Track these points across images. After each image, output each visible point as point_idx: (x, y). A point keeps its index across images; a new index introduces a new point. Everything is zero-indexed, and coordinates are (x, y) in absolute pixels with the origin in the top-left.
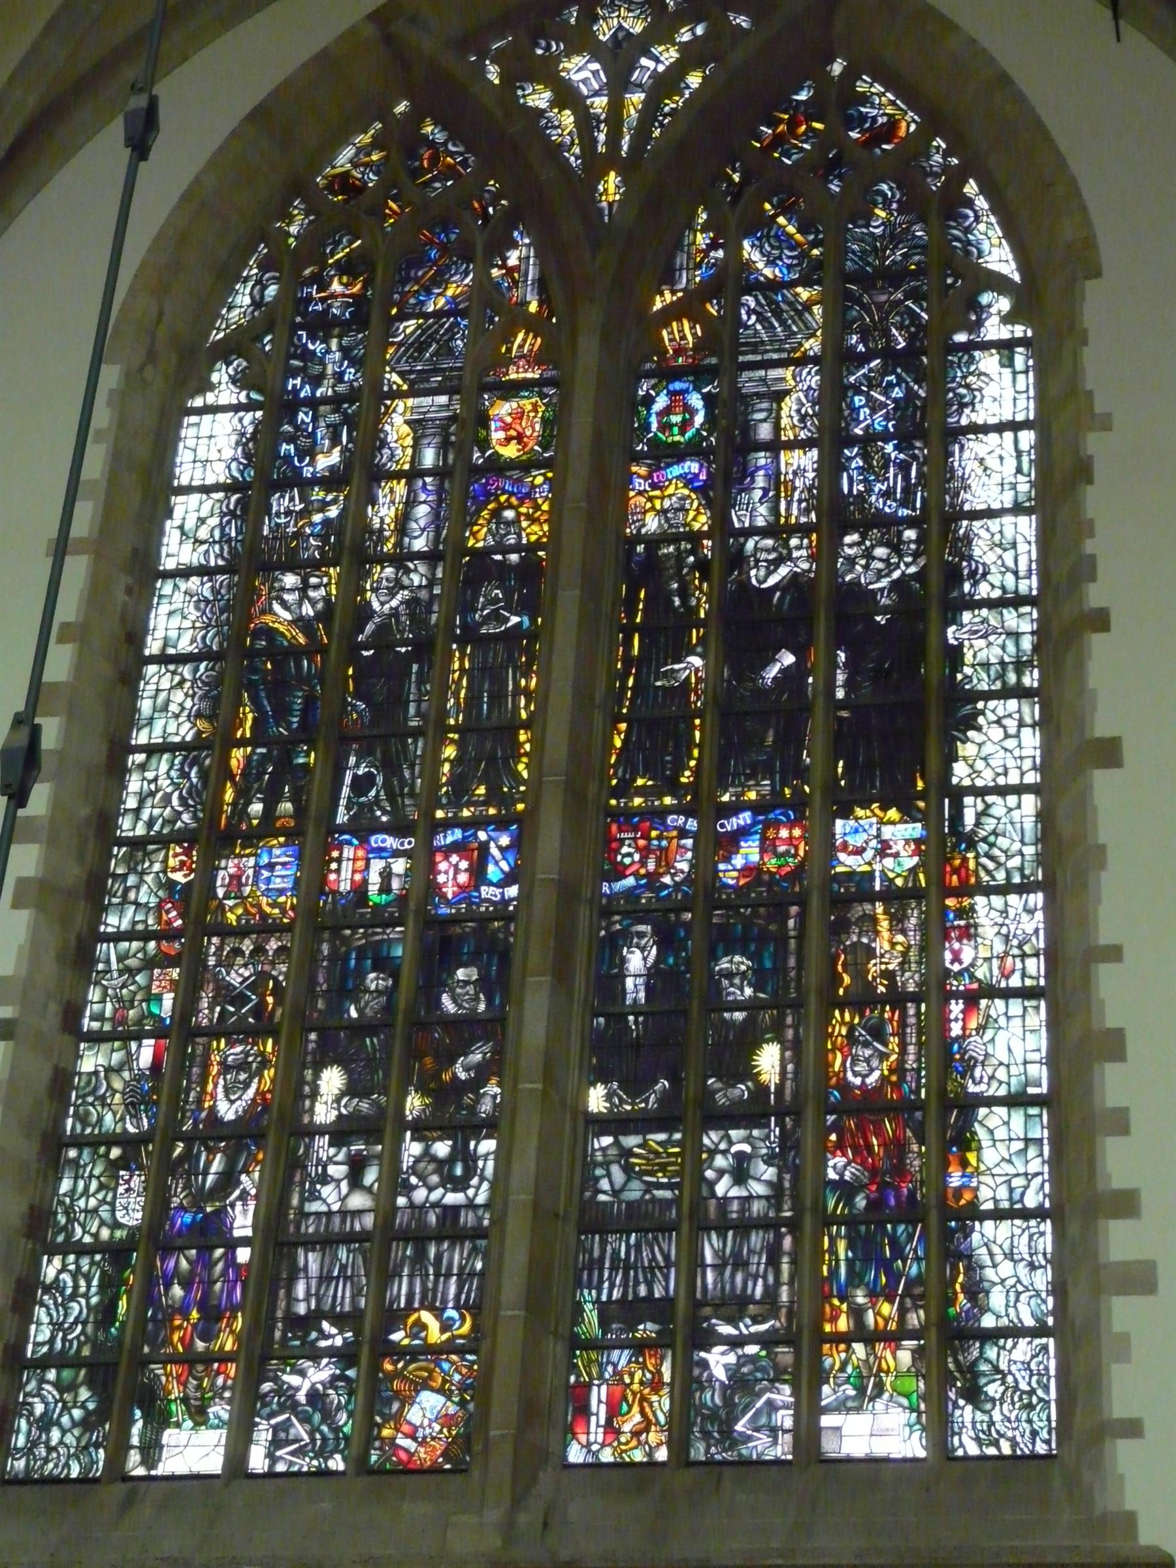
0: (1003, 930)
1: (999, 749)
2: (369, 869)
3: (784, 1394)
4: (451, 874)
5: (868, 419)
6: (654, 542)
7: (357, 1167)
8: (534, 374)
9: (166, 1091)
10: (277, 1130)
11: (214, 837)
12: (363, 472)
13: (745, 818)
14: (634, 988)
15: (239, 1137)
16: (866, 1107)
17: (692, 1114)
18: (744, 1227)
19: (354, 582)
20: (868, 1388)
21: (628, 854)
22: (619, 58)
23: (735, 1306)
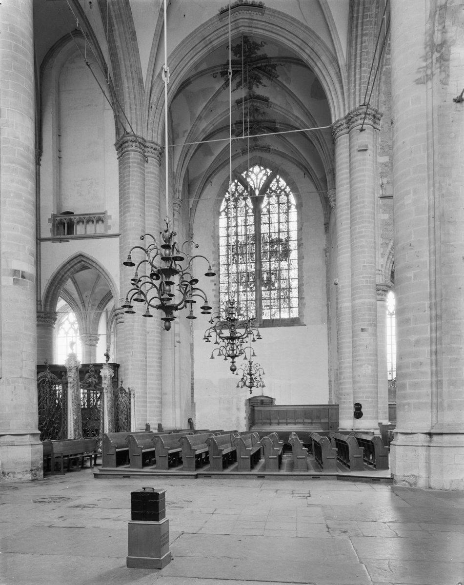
0: (294, 273)
1: (294, 255)
2: (242, 267)
3: (278, 313)
4: (249, 268)
5: (282, 220)
6: (264, 233)
7: (244, 294)
8: (252, 214)
9: (228, 288)
10: (238, 292)
11: (229, 265)
12: (237, 226)
13: (273, 262)
14: (265, 279)
15: (235, 292)
16: (284, 289)
17: (270, 290)
18: (275, 299)
19: (237, 238)
20: (284, 312)
21: (263, 265)
22: (257, 176)
23: (275, 306)
